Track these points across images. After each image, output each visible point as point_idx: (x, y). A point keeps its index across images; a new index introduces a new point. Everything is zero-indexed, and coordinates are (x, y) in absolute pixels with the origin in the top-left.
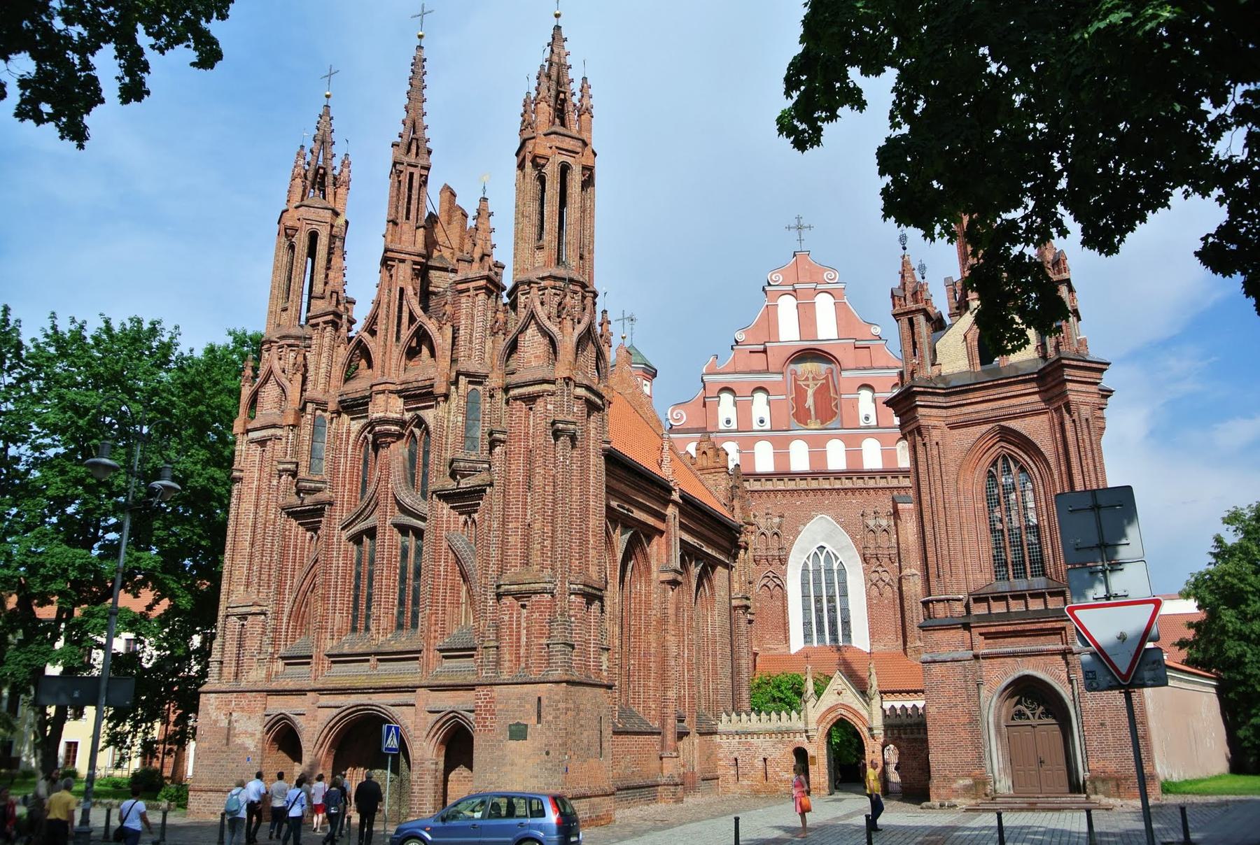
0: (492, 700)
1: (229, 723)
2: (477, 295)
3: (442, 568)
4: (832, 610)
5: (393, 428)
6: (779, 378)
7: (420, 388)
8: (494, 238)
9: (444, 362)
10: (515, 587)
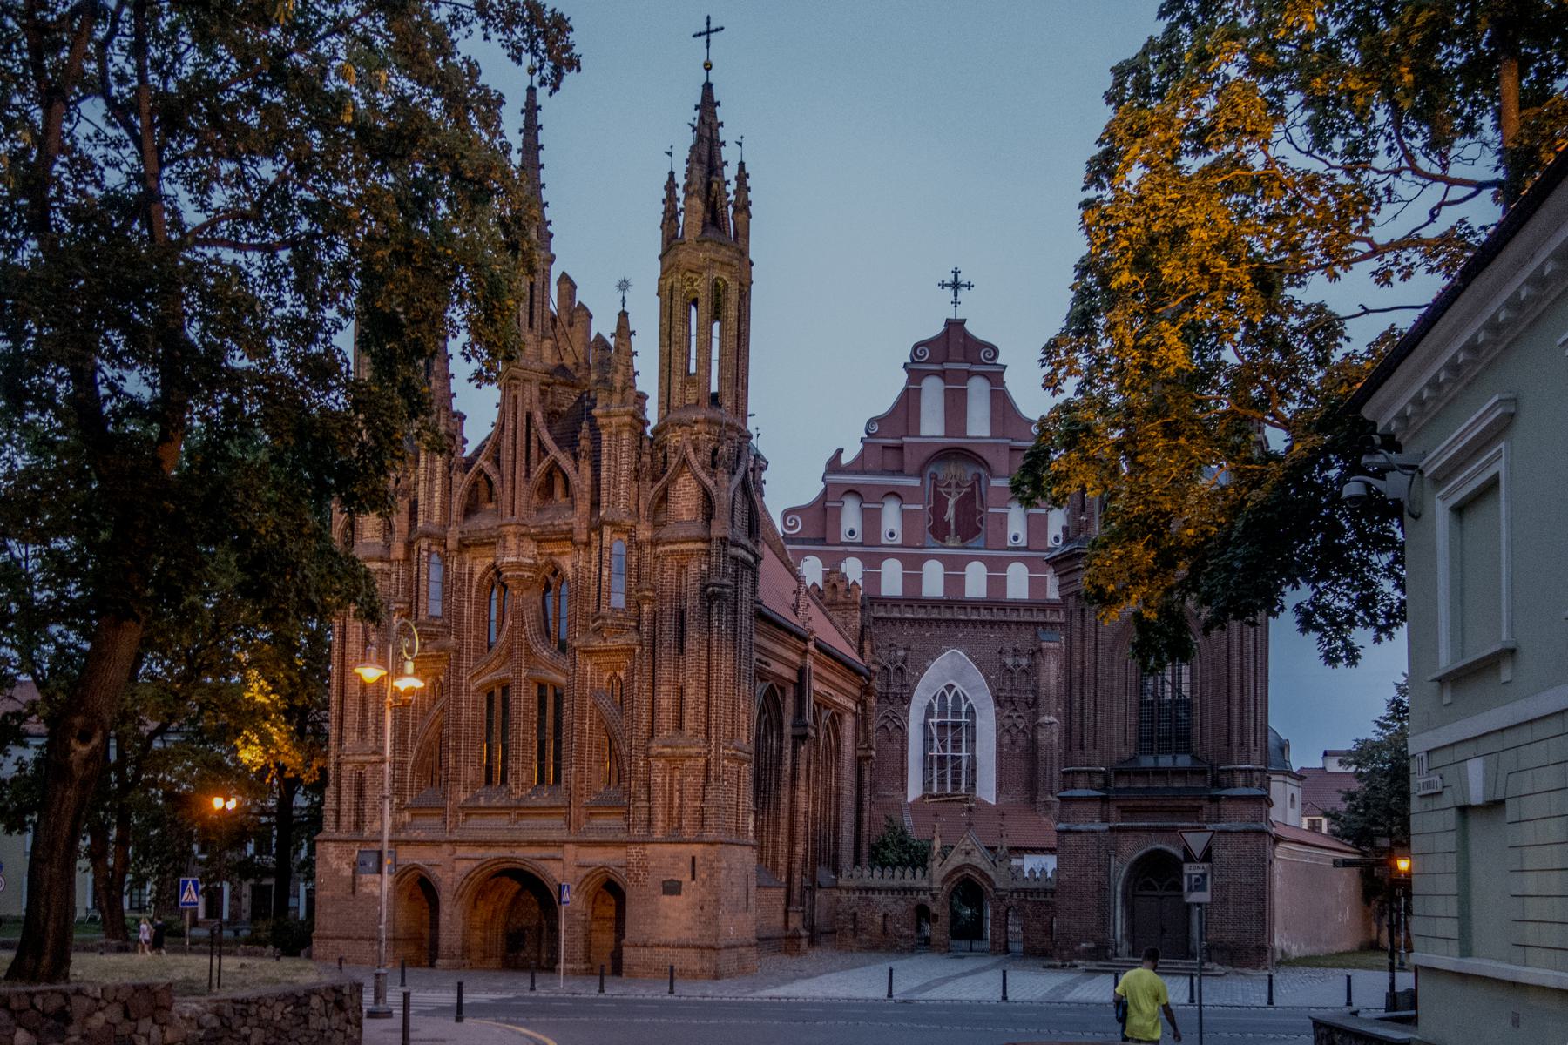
0: (645, 858)
5: (527, 574)
6: (916, 482)
9: (584, 506)
10: (669, 750)
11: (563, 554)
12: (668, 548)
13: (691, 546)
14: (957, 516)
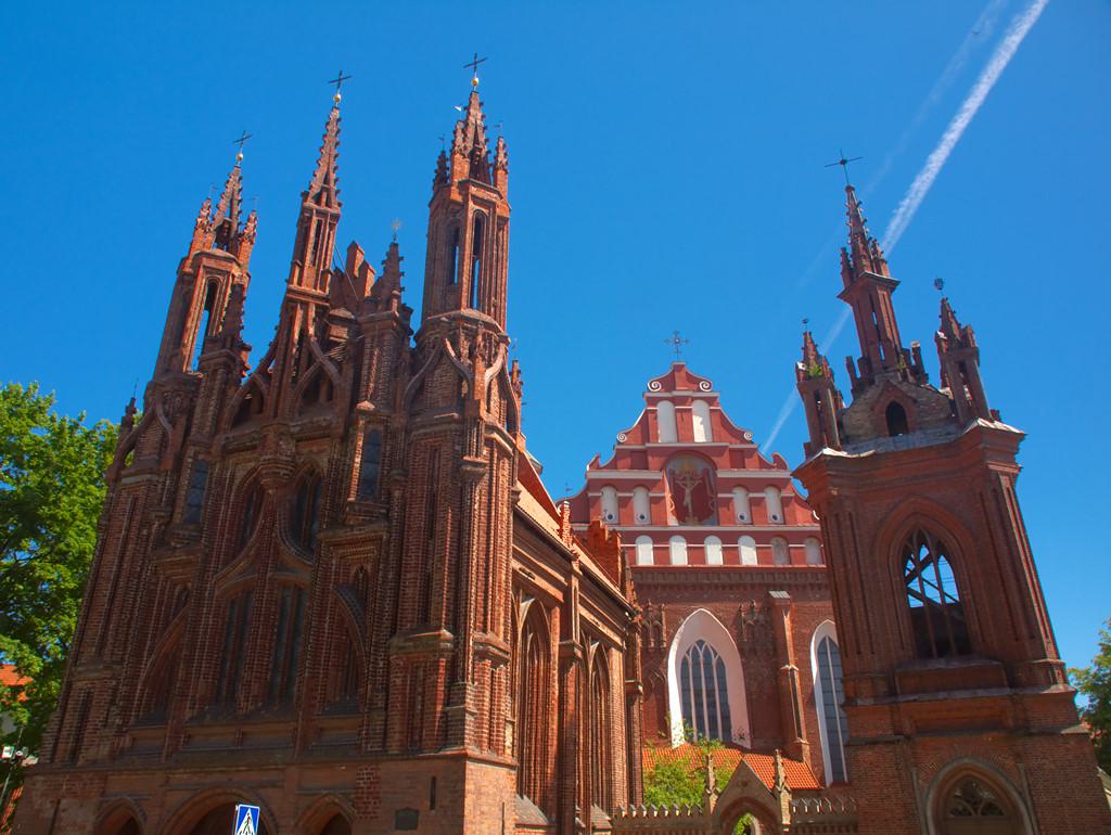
1: (56, 813)
2: (383, 335)
3: (326, 626)
4: (712, 705)
5: (282, 472)
8: (403, 282)
11: (321, 452)
12: (422, 431)
14: (692, 501)
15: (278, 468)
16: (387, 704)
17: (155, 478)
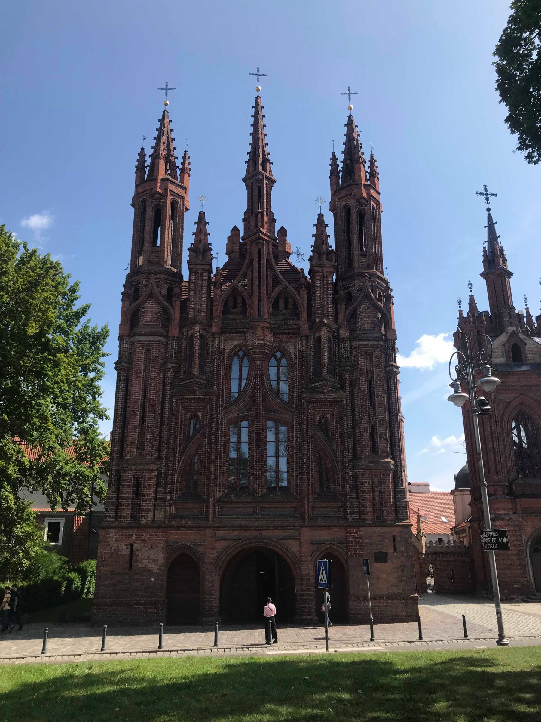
1: (132, 550)
2: (327, 276)
3: (310, 448)
7: (288, 329)
13: (376, 343)
15: (265, 349)
16: (358, 496)
17: (163, 339)
